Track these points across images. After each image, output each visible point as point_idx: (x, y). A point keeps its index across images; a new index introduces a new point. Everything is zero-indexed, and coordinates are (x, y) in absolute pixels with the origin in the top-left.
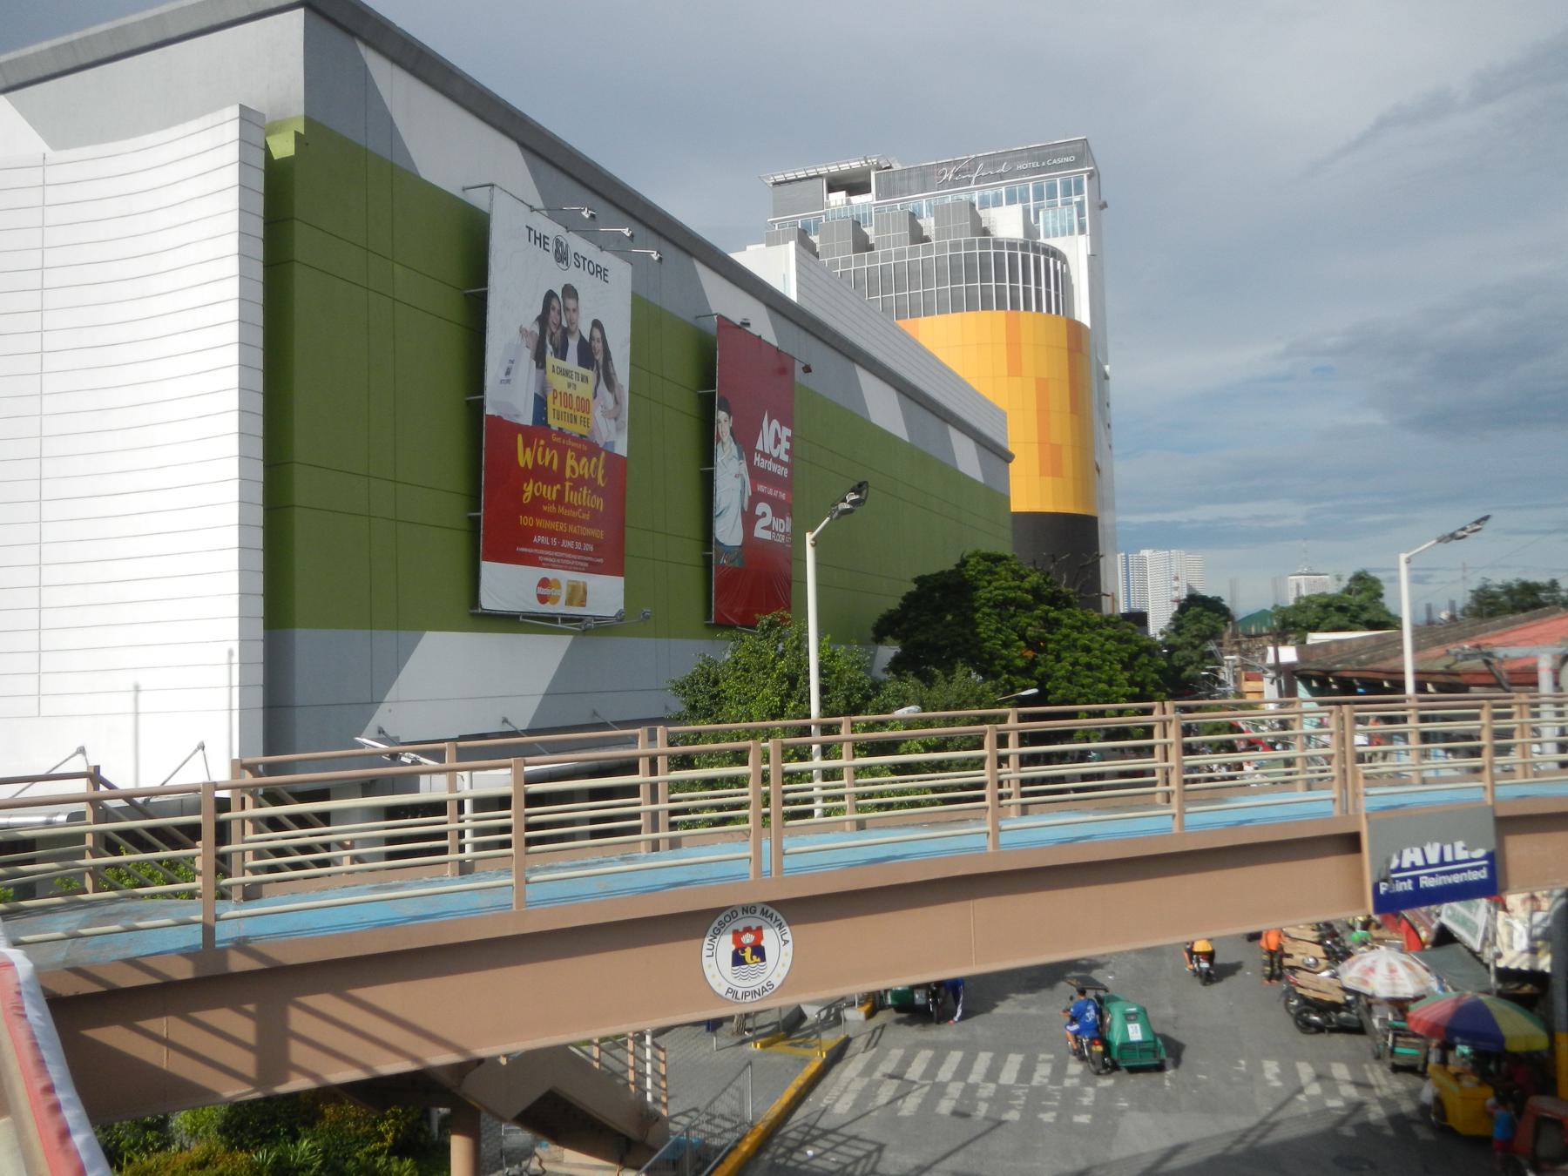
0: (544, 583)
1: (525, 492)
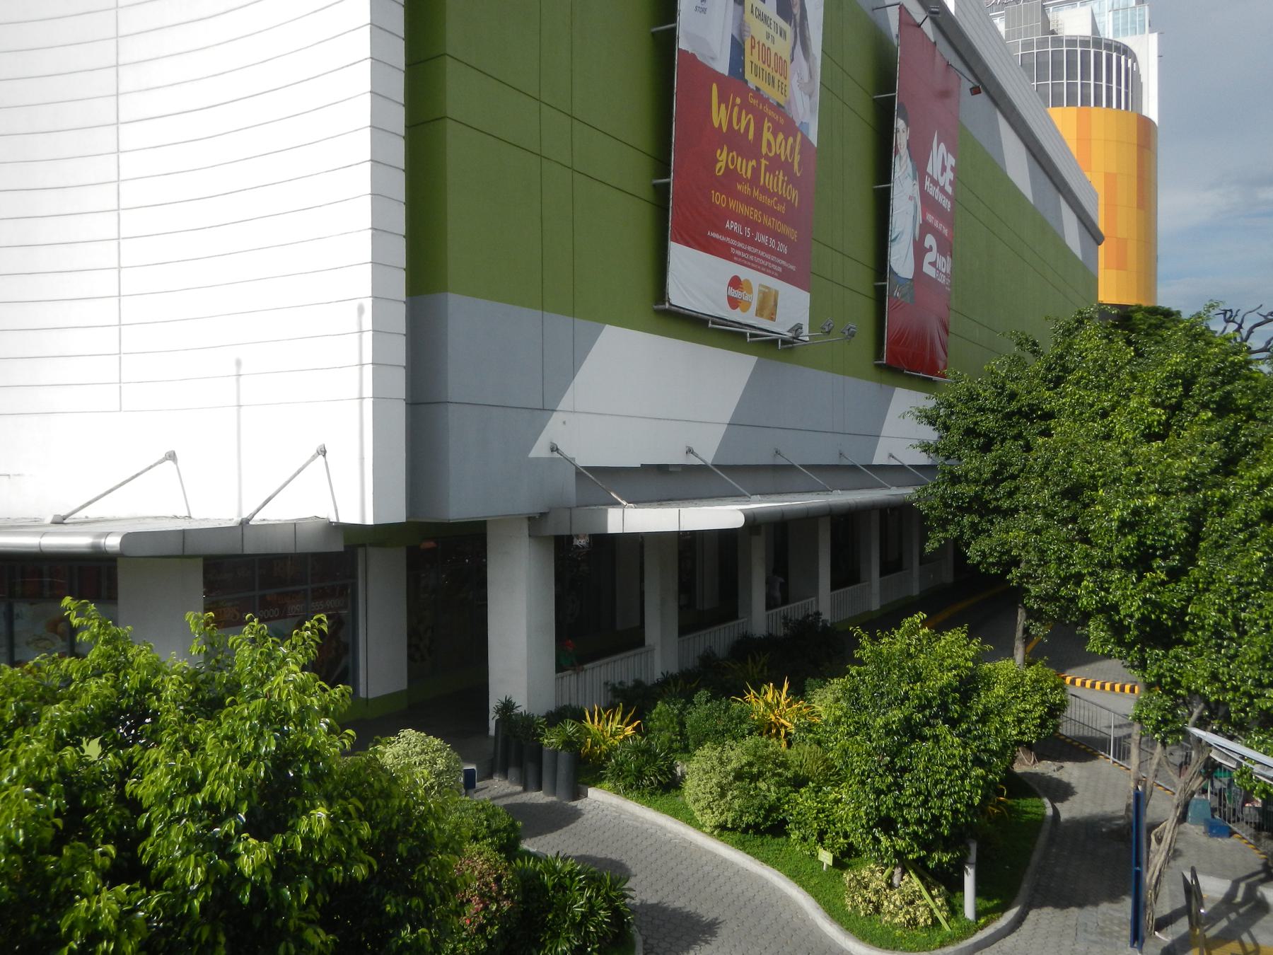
0: (735, 282)
1: (717, 161)
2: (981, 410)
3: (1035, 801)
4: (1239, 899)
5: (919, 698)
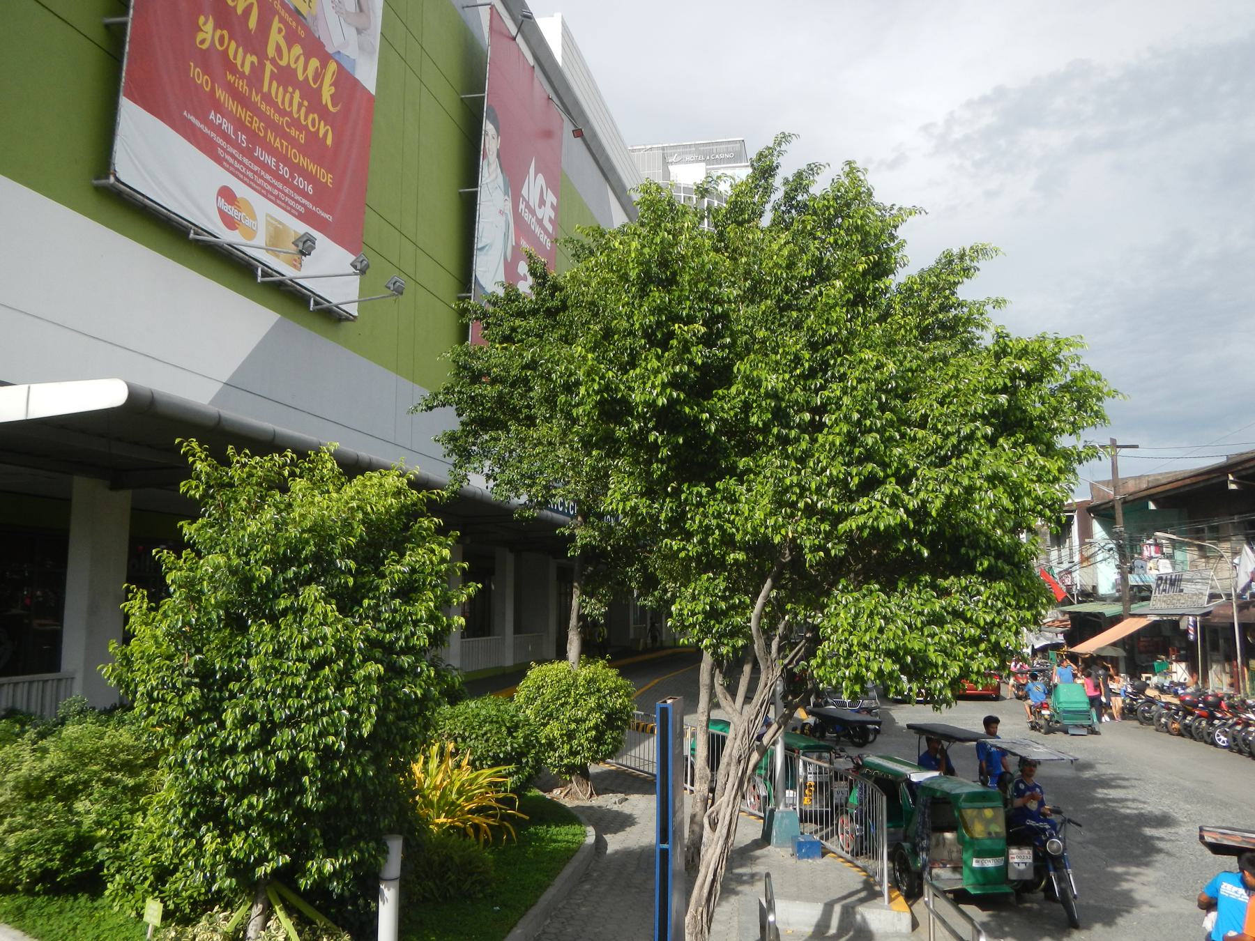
2: (521, 314)
3: (576, 829)
4: (833, 930)
5: (275, 542)
